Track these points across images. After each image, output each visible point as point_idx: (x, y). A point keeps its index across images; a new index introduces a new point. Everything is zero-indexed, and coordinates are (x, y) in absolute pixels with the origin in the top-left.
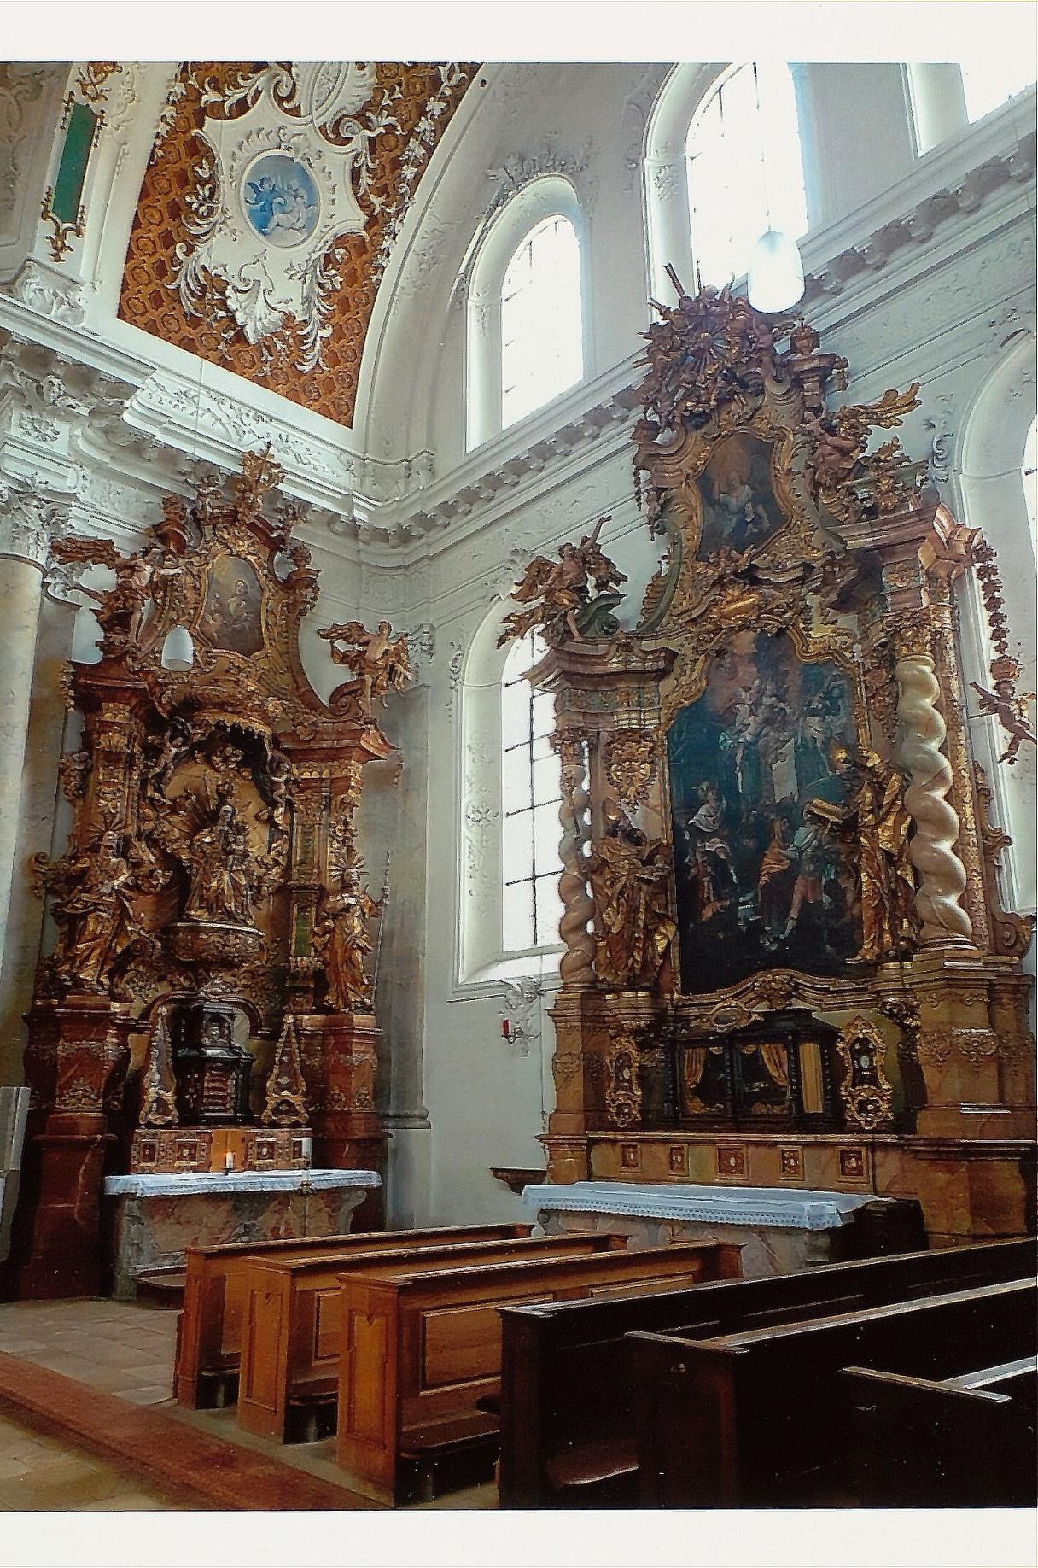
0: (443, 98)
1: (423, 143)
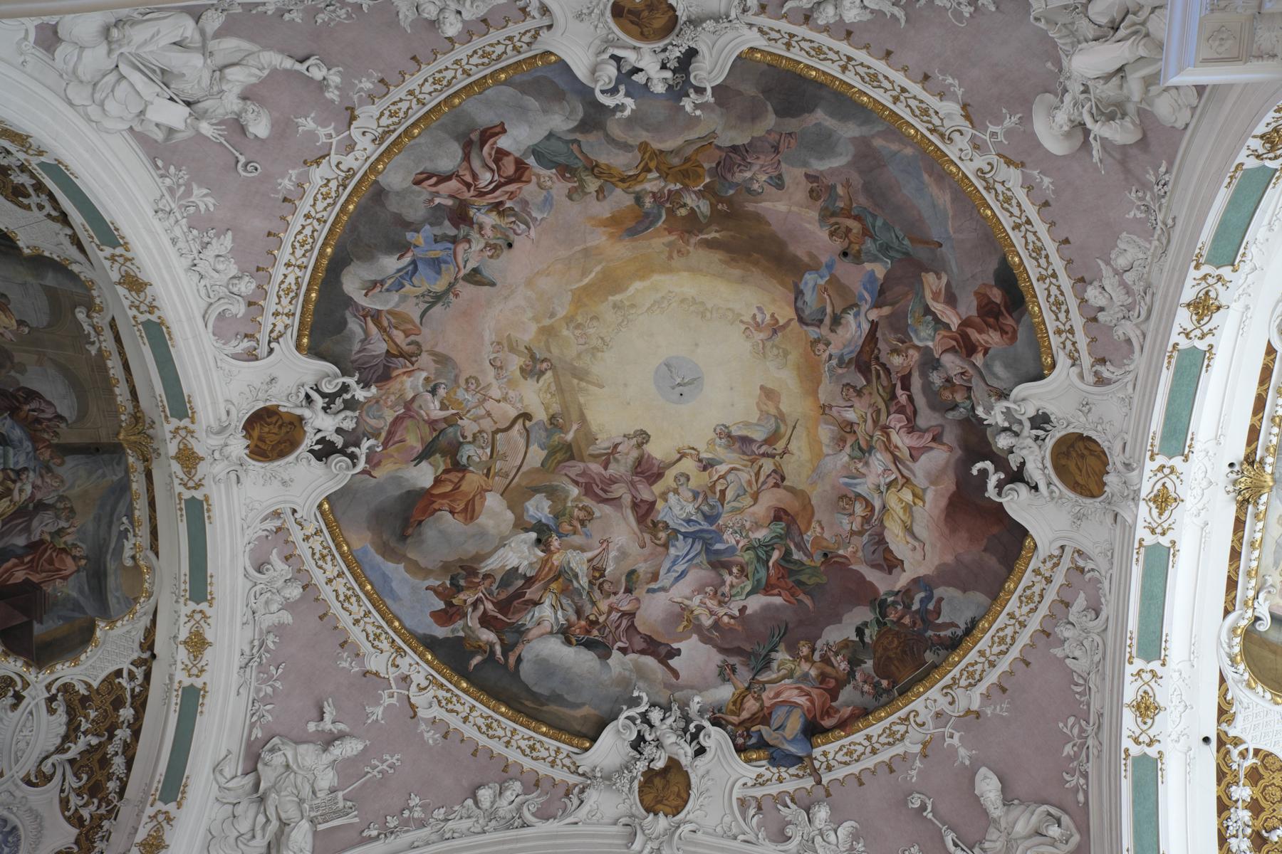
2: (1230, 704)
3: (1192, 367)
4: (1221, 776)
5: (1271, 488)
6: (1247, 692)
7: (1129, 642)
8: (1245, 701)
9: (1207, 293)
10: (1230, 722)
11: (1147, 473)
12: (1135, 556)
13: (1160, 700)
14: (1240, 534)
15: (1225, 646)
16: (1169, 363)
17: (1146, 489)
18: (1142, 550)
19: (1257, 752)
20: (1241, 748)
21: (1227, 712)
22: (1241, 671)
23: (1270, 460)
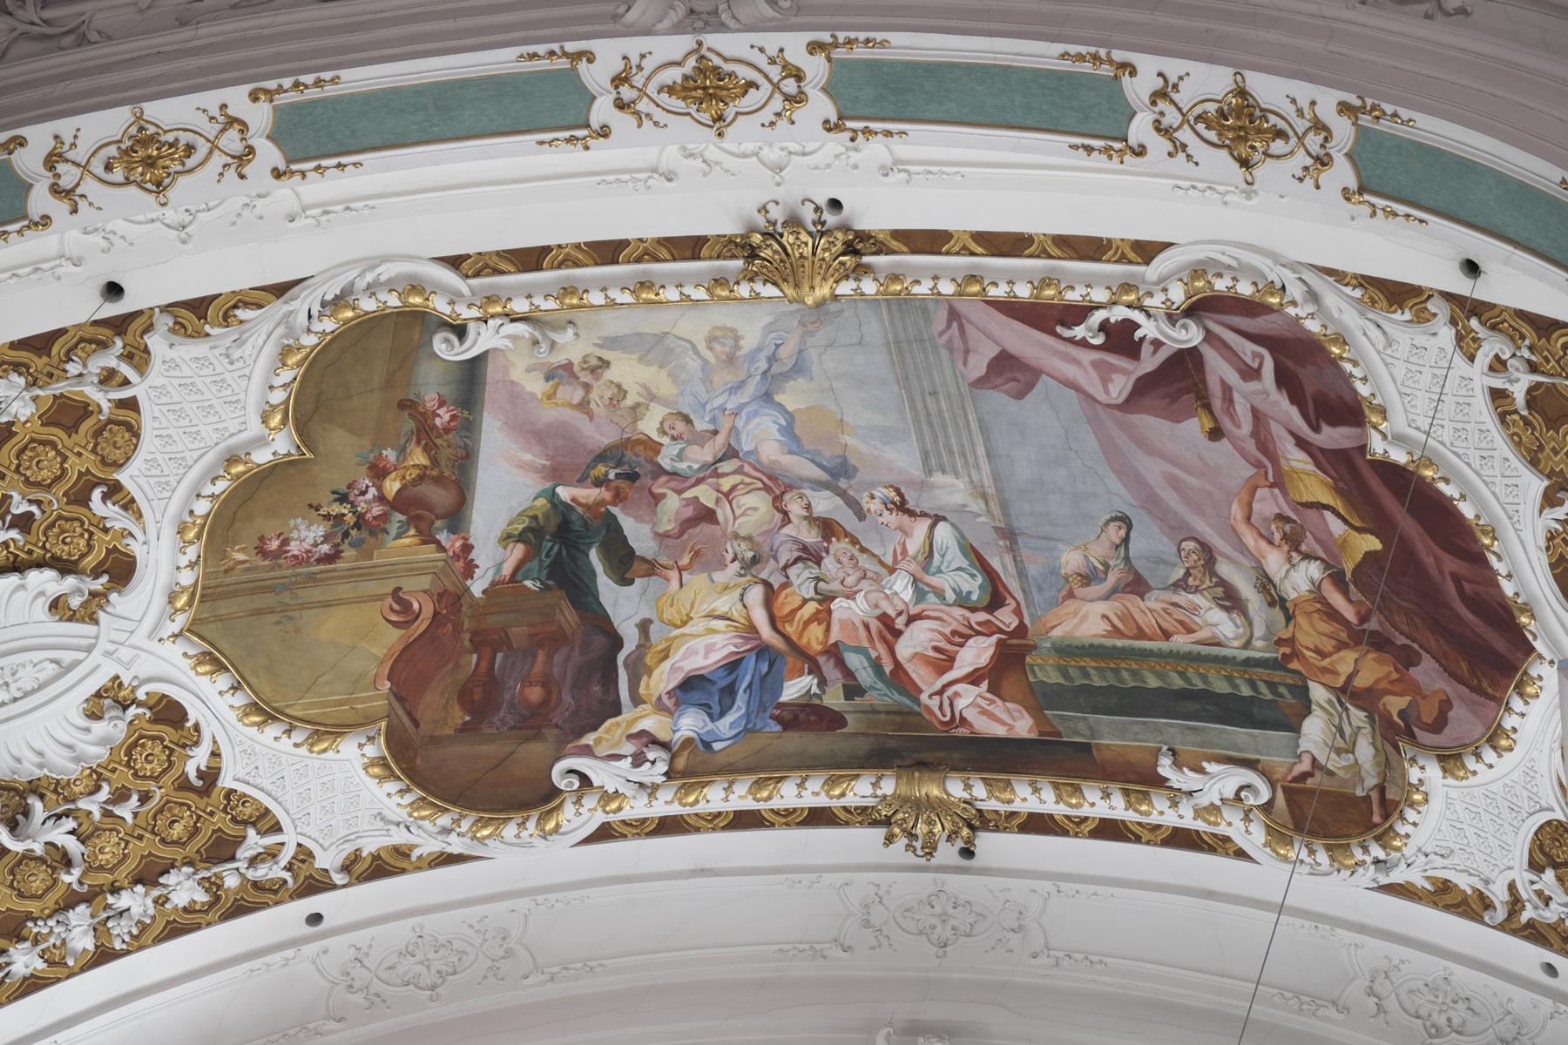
0: (213, 886)
1: (100, 929)
2: (226, 319)
3: (1084, 111)
4: (41, 344)
5: (801, 301)
6: (270, 350)
7: (308, 79)
8: (247, 350)
9: (1280, 134)
10: (180, 329)
11: (772, 41)
12: (542, 49)
13: (182, 190)
14: (664, 253)
15: (369, 277)
16: (1081, 58)
17: (728, 44)
18: (563, 64)
19: (131, 404)
20: (126, 370)
21: (202, 316)
22: (317, 326)
23: (869, 287)
